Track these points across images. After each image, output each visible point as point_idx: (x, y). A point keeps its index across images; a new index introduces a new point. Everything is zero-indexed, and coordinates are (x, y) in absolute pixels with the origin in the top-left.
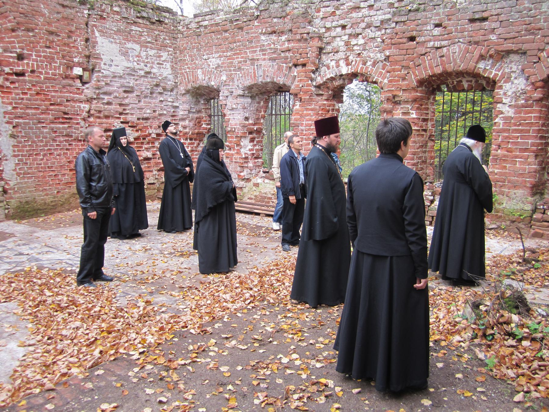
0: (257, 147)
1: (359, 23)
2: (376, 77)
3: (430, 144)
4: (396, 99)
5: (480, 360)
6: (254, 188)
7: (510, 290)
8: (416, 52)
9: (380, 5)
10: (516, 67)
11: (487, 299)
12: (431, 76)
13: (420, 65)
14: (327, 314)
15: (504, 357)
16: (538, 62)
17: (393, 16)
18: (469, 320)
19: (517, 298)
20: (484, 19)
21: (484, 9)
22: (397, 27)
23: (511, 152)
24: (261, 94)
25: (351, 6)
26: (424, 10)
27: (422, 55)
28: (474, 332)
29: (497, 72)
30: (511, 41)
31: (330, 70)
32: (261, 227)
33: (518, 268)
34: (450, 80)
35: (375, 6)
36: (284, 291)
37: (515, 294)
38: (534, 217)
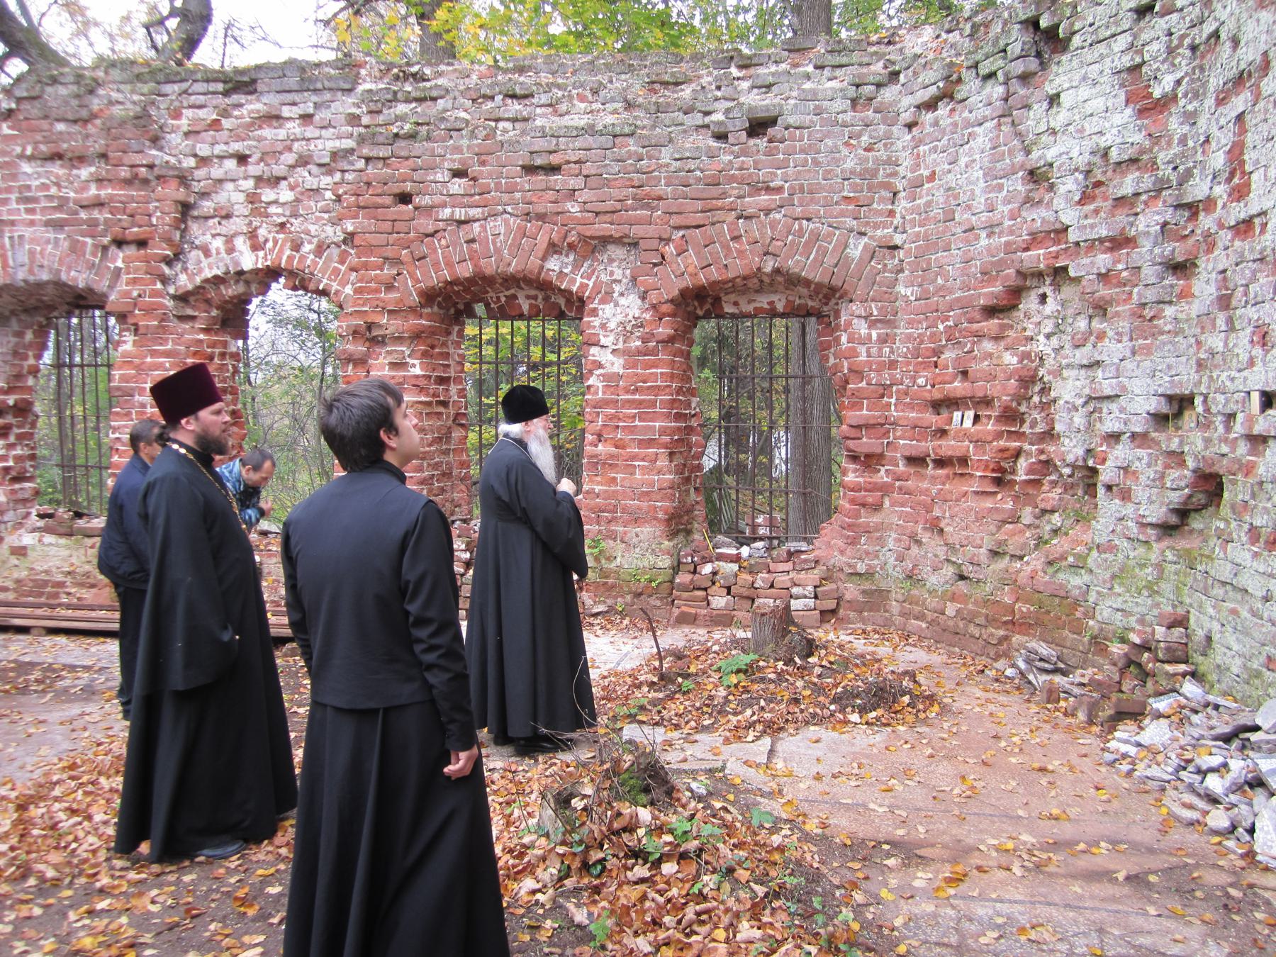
0: (18, 451)
1: (280, 153)
2: (325, 281)
3: (457, 434)
4: (375, 333)
5: (580, 927)
6: (14, 560)
7: (631, 752)
8: (415, 229)
9: (329, 116)
10: (620, 272)
11: (586, 780)
12: (451, 283)
13: (424, 258)
14: (208, 883)
15: (627, 909)
16: (661, 263)
17: (358, 144)
18: (552, 836)
19: (645, 770)
20: (554, 169)
21: (553, 148)
22: (370, 170)
23: (623, 448)
24: (26, 311)
25: (258, 111)
26: (428, 138)
27: (427, 235)
28: (563, 862)
29: (585, 281)
30: (608, 217)
31: (210, 260)
32: (32, 665)
33: (652, 695)
34: (492, 294)
35: (317, 118)
36: (91, 839)
37: (641, 760)
38: (677, 580)
